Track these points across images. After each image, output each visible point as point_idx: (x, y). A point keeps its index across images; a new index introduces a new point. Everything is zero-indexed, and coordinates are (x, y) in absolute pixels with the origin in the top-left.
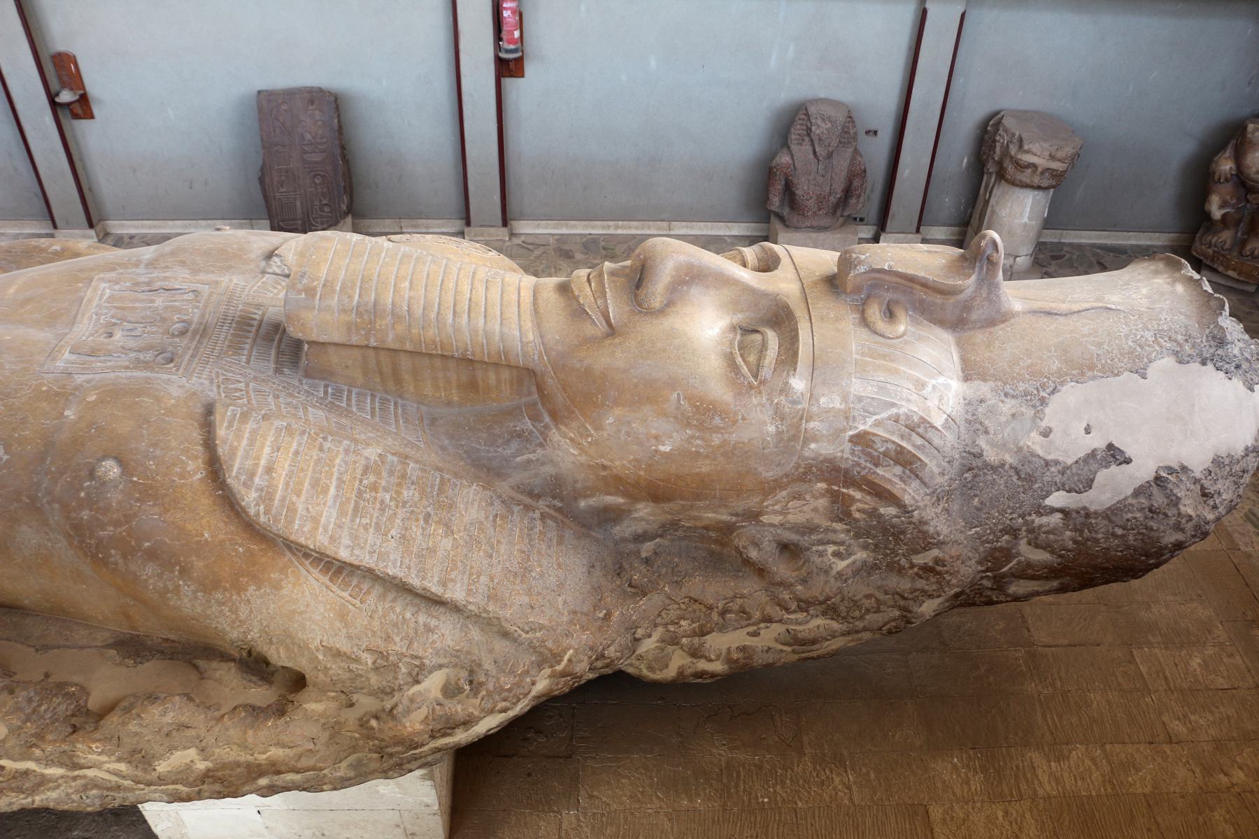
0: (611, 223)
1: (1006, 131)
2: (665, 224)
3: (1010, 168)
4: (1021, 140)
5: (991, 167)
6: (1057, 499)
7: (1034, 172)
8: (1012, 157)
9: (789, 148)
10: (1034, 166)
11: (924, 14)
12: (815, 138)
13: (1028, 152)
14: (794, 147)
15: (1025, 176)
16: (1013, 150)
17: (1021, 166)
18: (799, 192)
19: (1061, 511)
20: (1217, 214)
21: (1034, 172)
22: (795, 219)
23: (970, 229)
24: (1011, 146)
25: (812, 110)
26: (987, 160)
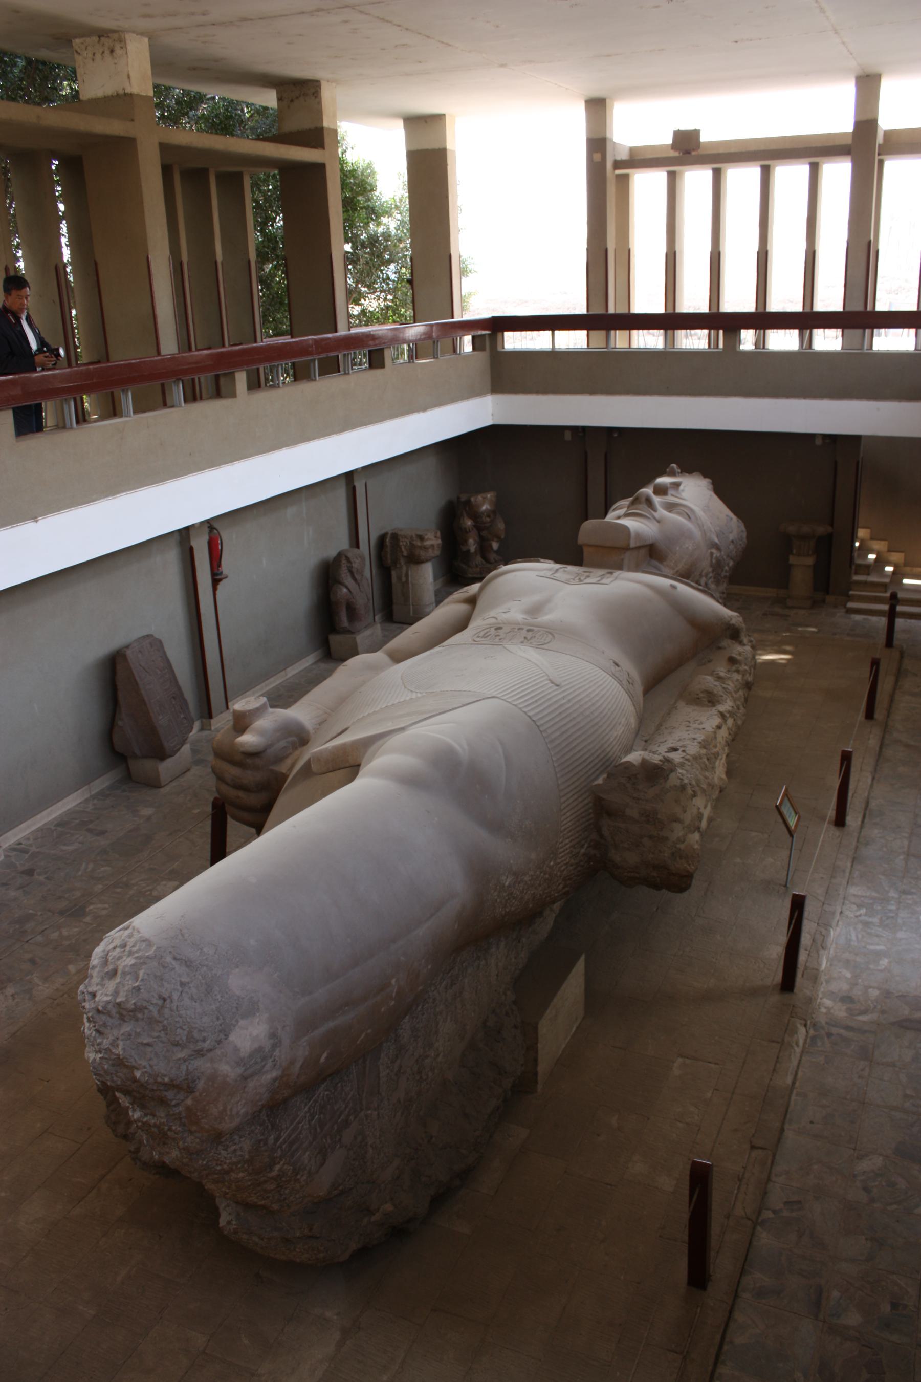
0: (263, 684)
1: (405, 537)
2: (283, 673)
3: (423, 554)
4: (421, 538)
5: (402, 561)
6: (731, 537)
8: (420, 547)
10: (432, 546)
12: (354, 570)
13: (428, 539)
16: (419, 543)
17: (425, 548)
19: (732, 541)
23: (395, 607)
24: (414, 542)
26: (395, 562)
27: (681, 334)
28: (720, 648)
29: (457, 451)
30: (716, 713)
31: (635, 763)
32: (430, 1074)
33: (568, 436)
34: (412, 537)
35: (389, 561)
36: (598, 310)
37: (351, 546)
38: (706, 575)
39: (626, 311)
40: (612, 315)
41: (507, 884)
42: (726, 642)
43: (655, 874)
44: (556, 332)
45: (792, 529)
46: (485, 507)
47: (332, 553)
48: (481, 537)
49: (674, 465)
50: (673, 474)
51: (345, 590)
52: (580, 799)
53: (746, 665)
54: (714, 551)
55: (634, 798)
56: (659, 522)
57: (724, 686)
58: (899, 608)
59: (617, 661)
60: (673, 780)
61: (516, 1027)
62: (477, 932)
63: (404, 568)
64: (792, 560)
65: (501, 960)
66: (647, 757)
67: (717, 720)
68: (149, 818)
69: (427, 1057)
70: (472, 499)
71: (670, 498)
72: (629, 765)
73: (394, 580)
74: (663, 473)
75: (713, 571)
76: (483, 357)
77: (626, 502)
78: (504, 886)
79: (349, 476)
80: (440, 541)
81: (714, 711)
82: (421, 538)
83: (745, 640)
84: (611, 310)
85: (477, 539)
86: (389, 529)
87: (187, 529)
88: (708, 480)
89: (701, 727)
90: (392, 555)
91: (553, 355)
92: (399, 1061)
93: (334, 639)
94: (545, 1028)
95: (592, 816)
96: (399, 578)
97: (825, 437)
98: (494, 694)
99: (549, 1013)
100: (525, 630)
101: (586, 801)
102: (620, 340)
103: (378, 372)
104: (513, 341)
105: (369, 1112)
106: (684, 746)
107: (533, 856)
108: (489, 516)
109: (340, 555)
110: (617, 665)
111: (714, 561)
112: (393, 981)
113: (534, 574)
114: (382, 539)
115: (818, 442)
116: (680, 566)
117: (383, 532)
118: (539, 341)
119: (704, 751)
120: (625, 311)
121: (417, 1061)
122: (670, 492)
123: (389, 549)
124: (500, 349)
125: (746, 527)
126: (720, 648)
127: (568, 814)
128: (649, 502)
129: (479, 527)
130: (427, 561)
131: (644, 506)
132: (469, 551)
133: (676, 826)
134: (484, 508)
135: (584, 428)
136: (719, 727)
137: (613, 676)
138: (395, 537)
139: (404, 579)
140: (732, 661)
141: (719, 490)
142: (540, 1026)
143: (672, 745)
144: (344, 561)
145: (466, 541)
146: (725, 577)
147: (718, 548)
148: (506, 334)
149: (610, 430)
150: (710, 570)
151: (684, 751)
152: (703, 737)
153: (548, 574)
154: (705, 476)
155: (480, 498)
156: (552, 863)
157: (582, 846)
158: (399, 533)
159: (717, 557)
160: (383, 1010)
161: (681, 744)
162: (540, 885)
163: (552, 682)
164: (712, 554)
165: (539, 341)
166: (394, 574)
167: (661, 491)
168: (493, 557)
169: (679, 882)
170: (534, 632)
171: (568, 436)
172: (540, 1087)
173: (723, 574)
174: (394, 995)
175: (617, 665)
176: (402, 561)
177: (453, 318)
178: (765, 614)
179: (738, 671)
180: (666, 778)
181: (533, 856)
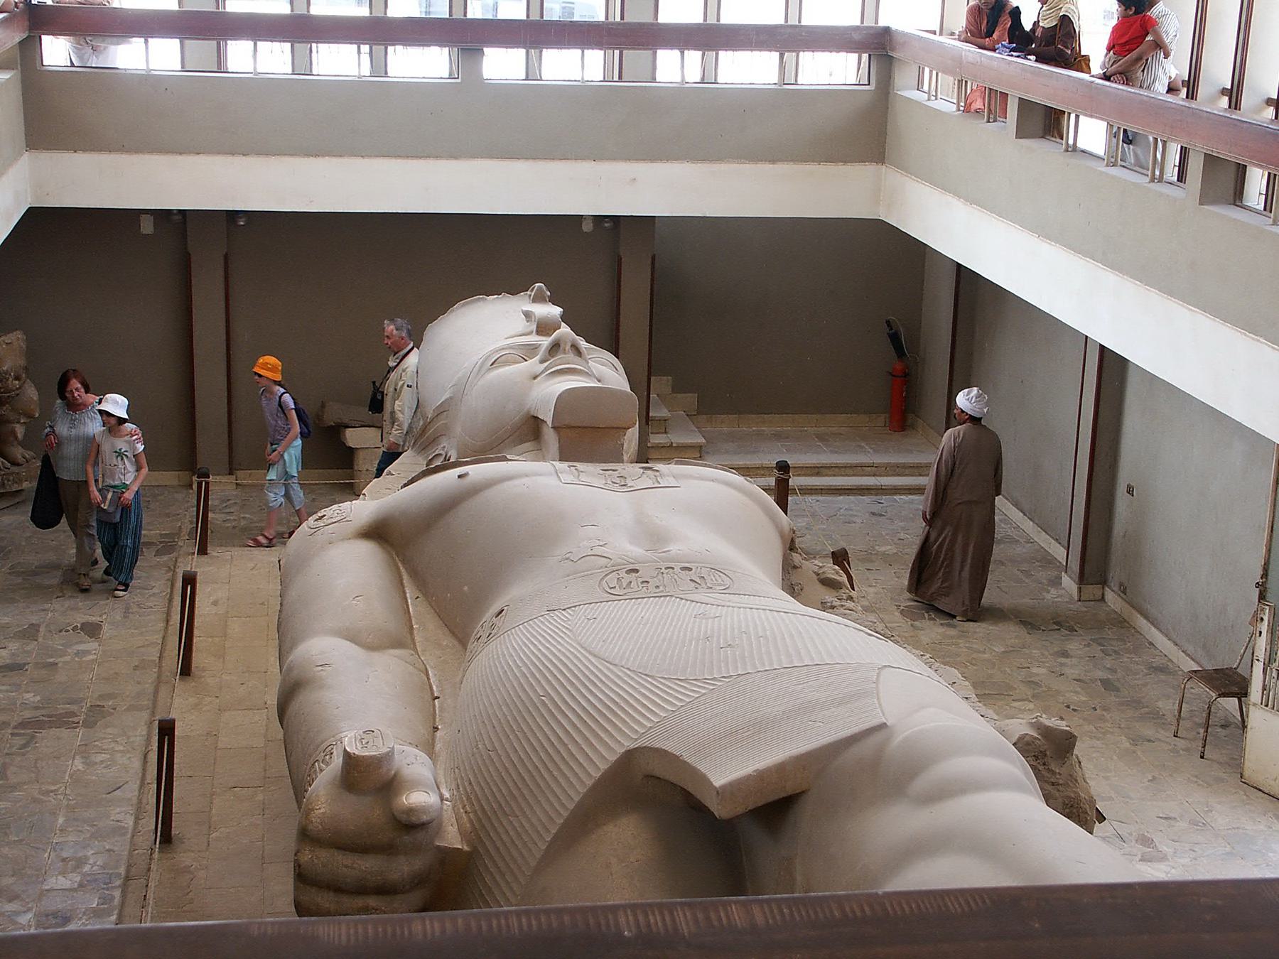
33: (147, 227)
50: (538, 299)
58: (794, 481)
97: (599, 219)
100: (677, 569)
108: (17, 378)
115: (587, 227)
126: (795, 567)
131: (571, 356)
149: (232, 215)
171: (147, 227)
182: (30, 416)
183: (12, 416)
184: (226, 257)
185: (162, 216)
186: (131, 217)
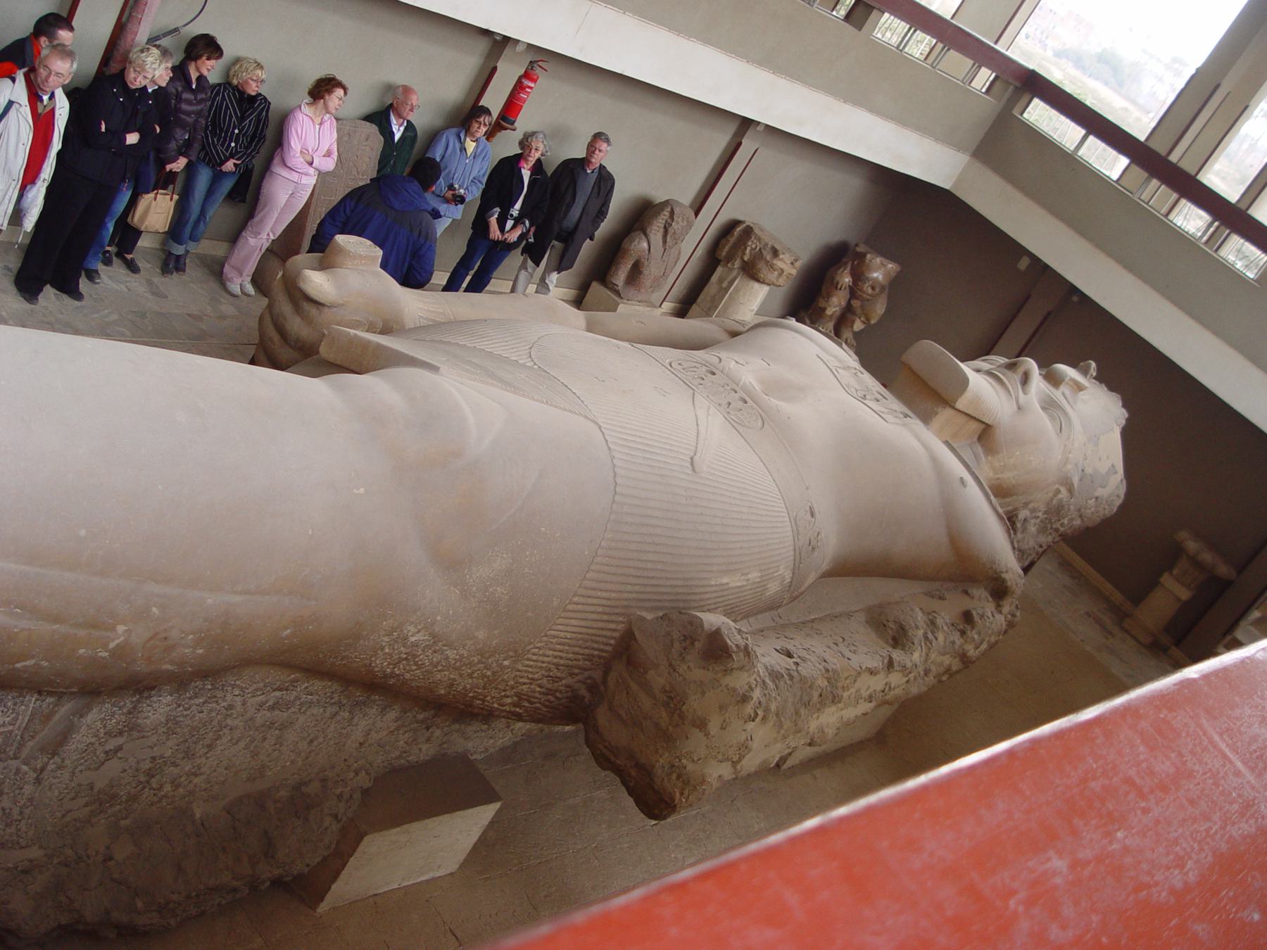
1: (759, 239)
3: (764, 273)
4: (775, 253)
6: (1100, 492)
7: (780, 275)
9: (646, 235)
10: (782, 271)
11: (739, 144)
12: (671, 231)
14: (652, 236)
15: (772, 276)
16: (768, 258)
17: (772, 267)
18: (646, 272)
20: (829, 312)
21: (780, 275)
22: (632, 292)
25: (677, 211)
26: (730, 258)
27: (1236, 241)
28: (966, 593)
29: (895, 194)
30: (885, 654)
31: (706, 626)
32: (167, 788)
33: (1024, 264)
34: (766, 245)
35: (724, 254)
36: (1160, 147)
37: (691, 206)
38: (1033, 511)
39: (1193, 173)
40: (1170, 162)
41: (413, 639)
42: (980, 593)
43: (633, 774)
44: (1091, 138)
45: (1192, 546)
46: (877, 275)
47: (659, 196)
48: (849, 303)
49: (1093, 365)
50: (1085, 372)
51: (645, 245)
52: (605, 617)
53: (979, 634)
54: (1063, 490)
55: (670, 665)
56: (1019, 408)
57: (930, 636)
59: (816, 511)
60: (740, 681)
61: (336, 817)
62: (333, 667)
63: (735, 273)
64: (1166, 579)
65: (376, 733)
66: (725, 631)
67: (875, 663)
68: (223, 317)
69: (175, 765)
70: (869, 256)
71: (1057, 394)
72: (696, 624)
73: (714, 278)
74: (1073, 365)
75: (1045, 513)
76: (991, 106)
77: (1002, 360)
78: (406, 638)
79: (746, 124)
80: (794, 272)
81: (886, 650)
82: (775, 253)
83: (1006, 609)
84: (1174, 158)
85: (844, 303)
86: (748, 218)
87: (506, 40)
88: (1124, 411)
89: (848, 654)
90: (732, 250)
91: (1070, 161)
92: (120, 741)
93: (596, 287)
94: (375, 845)
95: (609, 648)
96: (721, 280)
98: (600, 421)
99: (394, 834)
101: (612, 626)
102: (1156, 194)
103: (849, 28)
104: (1039, 114)
105: (25, 768)
106: (804, 660)
107: (481, 635)
108: (873, 288)
109: (667, 203)
110: (812, 515)
111: (1055, 502)
112: (121, 628)
113: (815, 349)
114: (734, 224)
116: (1009, 477)
117: (741, 218)
118: (1066, 132)
119: (822, 683)
120: (1191, 170)
121: (154, 758)
122: (1063, 388)
123: (732, 240)
124: (1016, 112)
125: (1128, 494)
126: (966, 593)
127: (573, 622)
128: (1026, 379)
129: (853, 292)
130: (763, 283)
131: (1017, 377)
132: (824, 309)
133: (696, 735)
134: (875, 275)
135: (1046, 267)
136: (872, 672)
137: (795, 522)
138: (748, 231)
139: (725, 285)
140: (967, 617)
141: (1130, 436)
142: (367, 839)
143: (790, 647)
144: (666, 213)
145: (829, 296)
146: (1057, 530)
147: (1070, 490)
148: (1036, 101)
149: (1074, 290)
150: (1043, 508)
151: (797, 664)
152: (838, 667)
153: (833, 363)
154: (1124, 406)
155: (879, 260)
156: (506, 663)
157: (571, 675)
158: (756, 231)
159: (1061, 500)
160: (82, 651)
161: (804, 654)
162: (470, 676)
163: (692, 464)
164: (1058, 491)
165: (1066, 132)
166: (720, 270)
167: (1054, 380)
168: (847, 334)
169: (655, 803)
170: (744, 407)
171: (1024, 264)
172: (323, 907)
173: (1057, 525)
174: (112, 645)
175: (812, 515)
176: (737, 264)
177: (996, 42)
178: (1088, 614)
179: (963, 633)
180: (728, 672)
181: (481, 635)
182: (868, 320)
183: (859, 311)
184: (1049, 313)
185: (1035, 260)
186: (1015, 249)
